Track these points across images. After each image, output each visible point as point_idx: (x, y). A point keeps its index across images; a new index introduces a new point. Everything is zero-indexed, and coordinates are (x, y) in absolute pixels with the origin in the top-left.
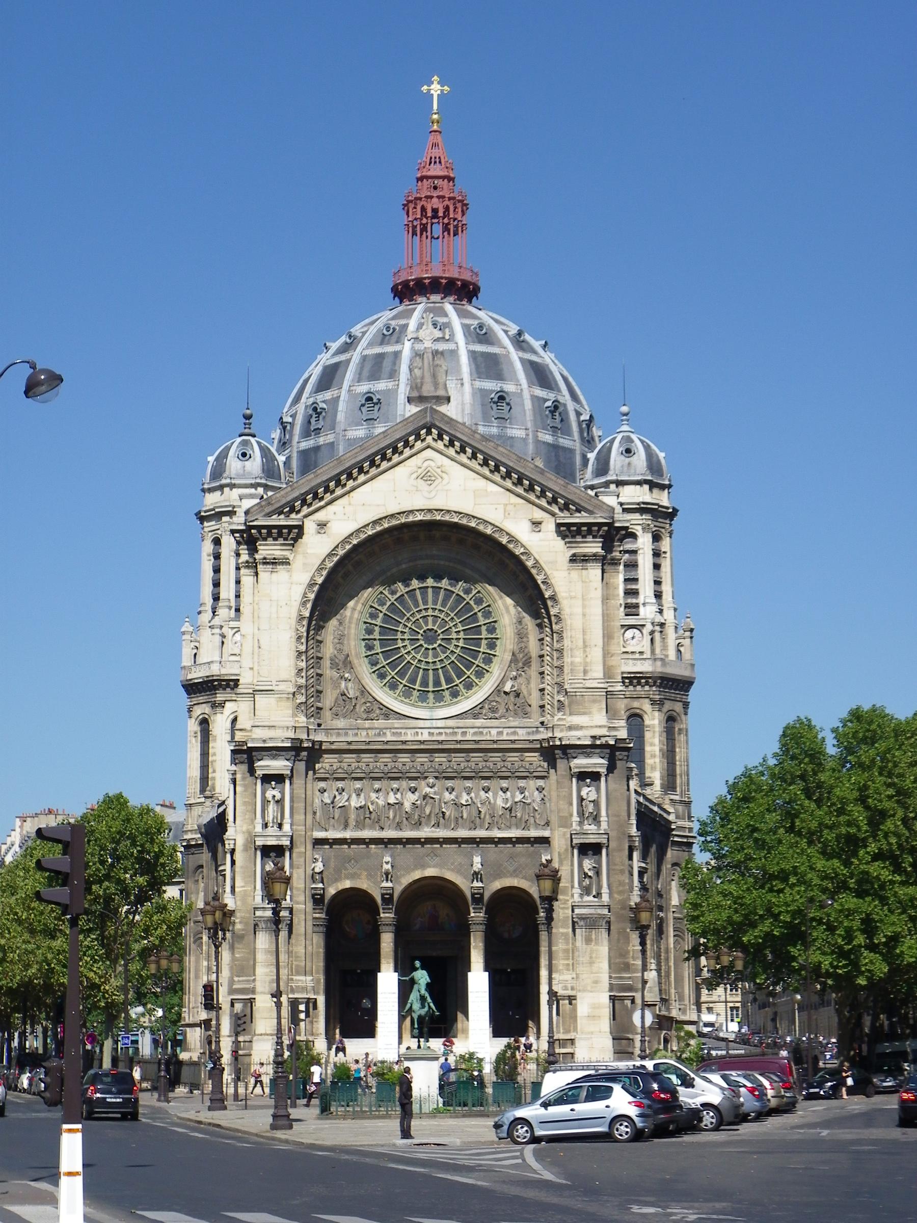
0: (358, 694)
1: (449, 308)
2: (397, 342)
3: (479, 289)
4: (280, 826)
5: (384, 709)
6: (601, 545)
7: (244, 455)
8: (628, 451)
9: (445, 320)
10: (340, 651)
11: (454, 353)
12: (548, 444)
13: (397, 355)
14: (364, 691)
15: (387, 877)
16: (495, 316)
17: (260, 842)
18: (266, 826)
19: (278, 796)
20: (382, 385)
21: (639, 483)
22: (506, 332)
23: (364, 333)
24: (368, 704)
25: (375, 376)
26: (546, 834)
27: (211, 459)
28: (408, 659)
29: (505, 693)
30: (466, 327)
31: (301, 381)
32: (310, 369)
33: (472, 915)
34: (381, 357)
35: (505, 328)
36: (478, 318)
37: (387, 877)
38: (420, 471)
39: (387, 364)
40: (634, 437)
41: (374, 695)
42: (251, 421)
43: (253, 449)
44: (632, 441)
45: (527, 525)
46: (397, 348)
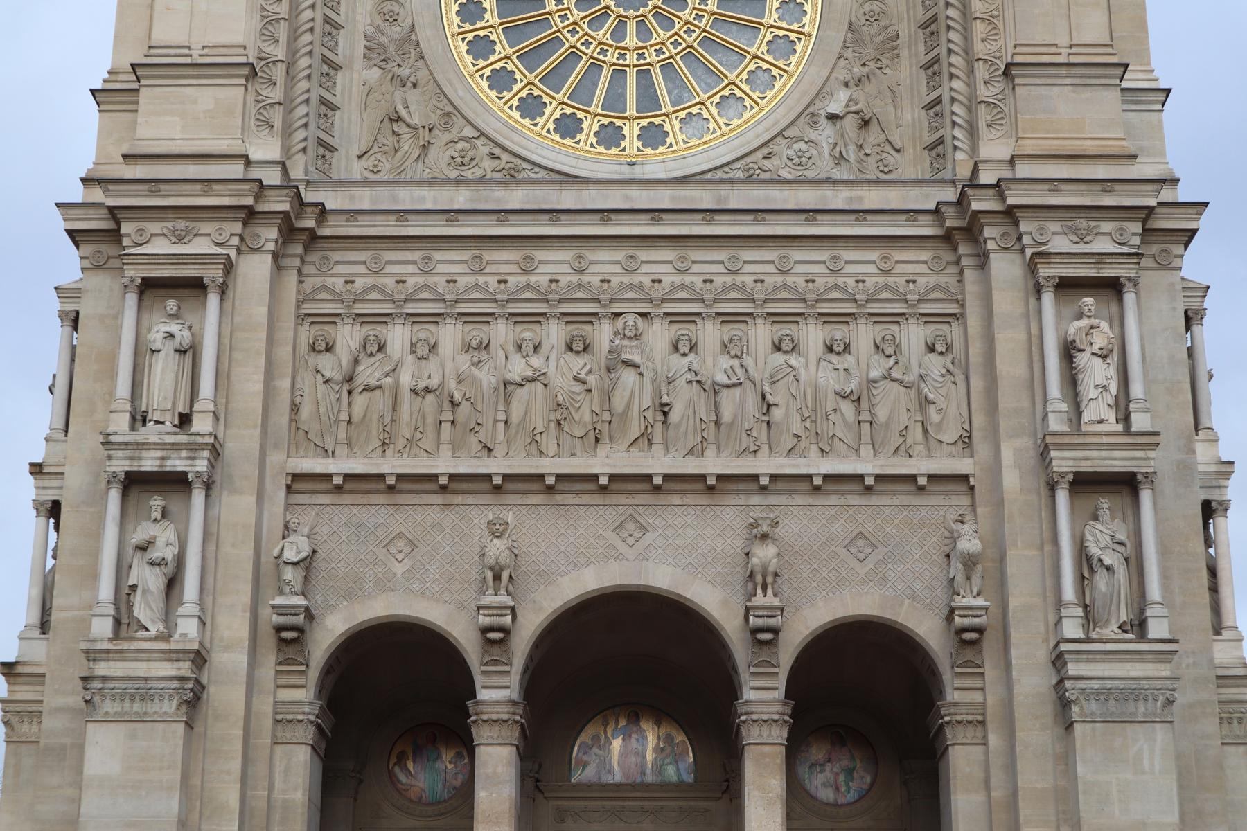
0: (434, 119)
4: (185, 420)
5: (505, 157)
10: (393, 18)
14: (451, 114)
15: (497, 578)
17: (121, 465)
18: (139, 419)
19: (183, 337)
24: (461, 145)
26: (963, 465)
28: (573, 40)
29: (833, 117)
33: (749, 694)
37: (497, 578)
41: (479, 122)
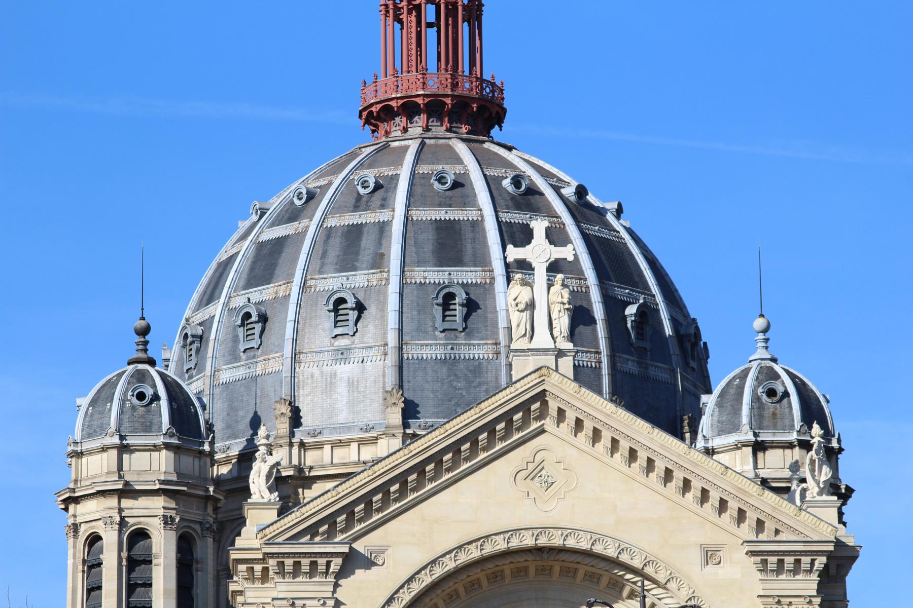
1: (461, 149)
2: (383, 206)
3: (504, 111)
6: (816, 587)
7: (141, 396)
8: (771, 393)
9: (459, 169)
11: (477, 226)
12: (632, 375)
13: (383, 228)
16: (527, 157)
20: (360, 279)
21: (790, 446)
22: (557, 189)
23: (324, 188)
25: (347, 264)
27: (84, 402)
30: (492, 184)
31: (214, 265)
32: (229, 243)
34: (354, 233)
35: (554, 181)
36: (514, 167)
38: (531, 467)
39: (367, 242)
40: (777, 368)
42: (147, 338)
43: (154, 386)
44: (777, 377)
45: (696, 556)
46: (383, 216)
